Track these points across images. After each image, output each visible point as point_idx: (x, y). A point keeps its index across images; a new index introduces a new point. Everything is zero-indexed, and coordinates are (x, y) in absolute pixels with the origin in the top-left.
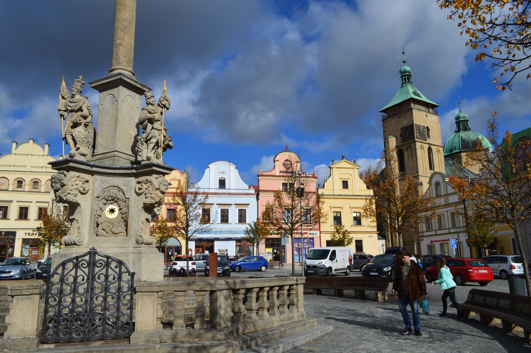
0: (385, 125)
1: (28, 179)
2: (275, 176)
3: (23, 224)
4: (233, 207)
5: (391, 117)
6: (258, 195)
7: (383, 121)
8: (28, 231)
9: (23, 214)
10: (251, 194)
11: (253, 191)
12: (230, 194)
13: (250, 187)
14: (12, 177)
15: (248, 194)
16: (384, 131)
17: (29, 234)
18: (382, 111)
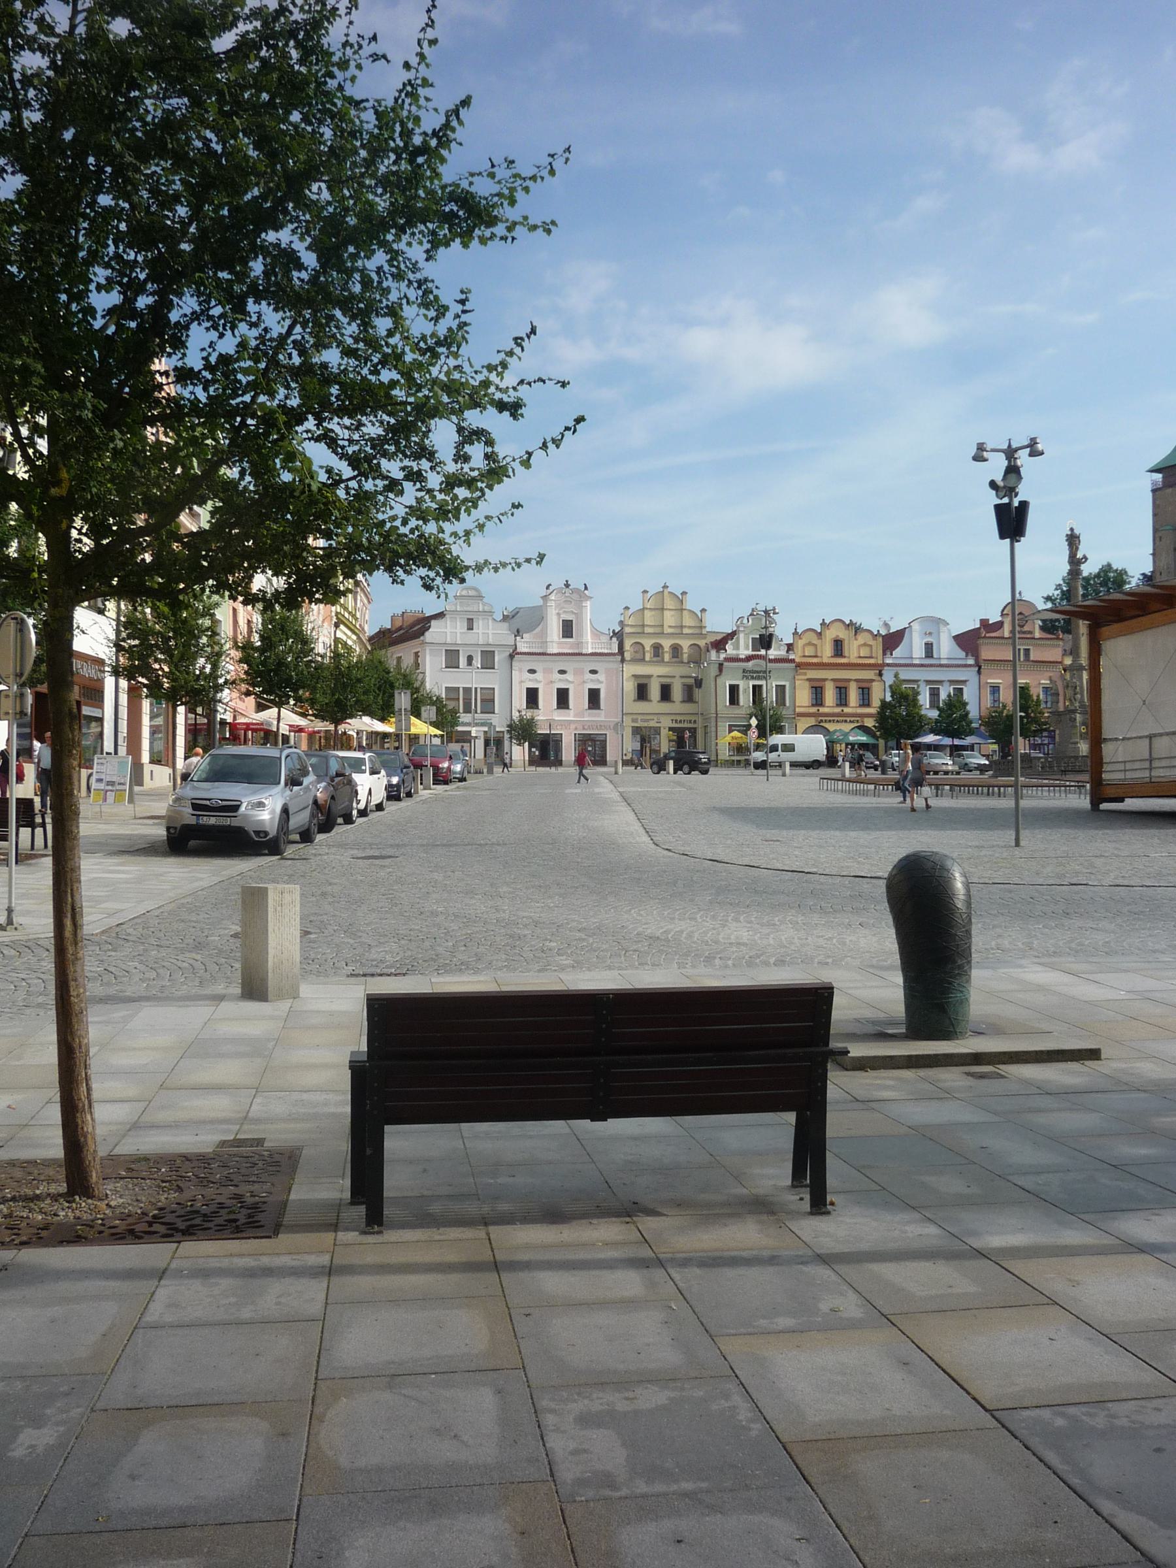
0: (1158, 502)
1: (667, 644)
2: (1003, 638)
3: (665, 707)
4: (946, 684)
5: (1170, 486)
6: (980, 667)
7: (1154, 491)
8: (674, 717)
9: (666, 693)
10: (970, 666)
11: (971, 661)
12: (941, 666)
13: (967, 656)
14: (648, 644)
15: (966, 666)
16: (1155, 515)
17: (676, 721)
18: (1152, 471)
